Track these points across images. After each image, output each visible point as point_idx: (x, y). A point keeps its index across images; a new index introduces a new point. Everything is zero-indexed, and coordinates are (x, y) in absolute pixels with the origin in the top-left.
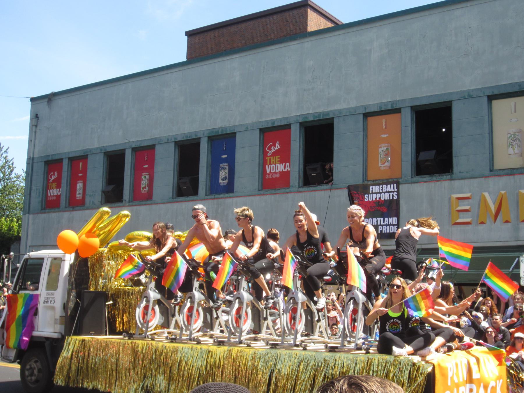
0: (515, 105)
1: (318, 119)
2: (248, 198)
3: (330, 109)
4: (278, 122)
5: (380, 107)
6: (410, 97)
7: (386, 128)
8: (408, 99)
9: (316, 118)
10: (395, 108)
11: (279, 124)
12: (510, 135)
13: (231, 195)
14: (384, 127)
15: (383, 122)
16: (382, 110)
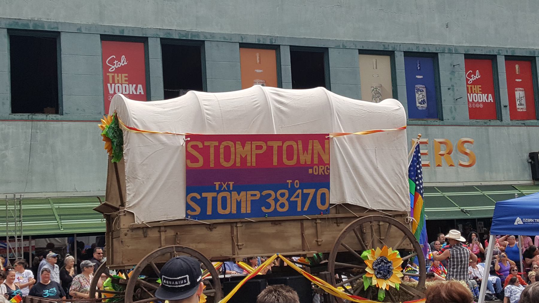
0: (376, 62)
1: (184, 38)
2: (88, 123)
3: (199, 30)
4: (129, 31)
5: (259, 40)
6: (288, 36)
7: (260, 63)
8: (287, 37)
9: (183, 37)
10: (274, 44)
11: (131, 34)
12: (372, 88)
13: (59, 117)
14: (258, 61)
15: (256, 57)
16: (261, 43)
